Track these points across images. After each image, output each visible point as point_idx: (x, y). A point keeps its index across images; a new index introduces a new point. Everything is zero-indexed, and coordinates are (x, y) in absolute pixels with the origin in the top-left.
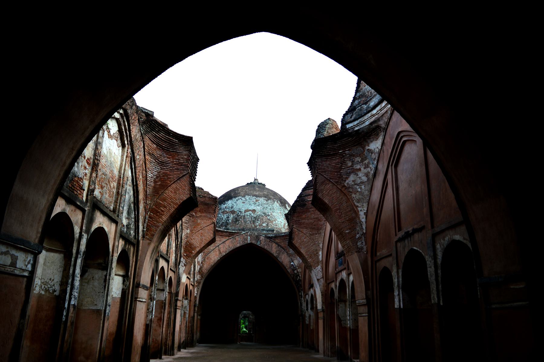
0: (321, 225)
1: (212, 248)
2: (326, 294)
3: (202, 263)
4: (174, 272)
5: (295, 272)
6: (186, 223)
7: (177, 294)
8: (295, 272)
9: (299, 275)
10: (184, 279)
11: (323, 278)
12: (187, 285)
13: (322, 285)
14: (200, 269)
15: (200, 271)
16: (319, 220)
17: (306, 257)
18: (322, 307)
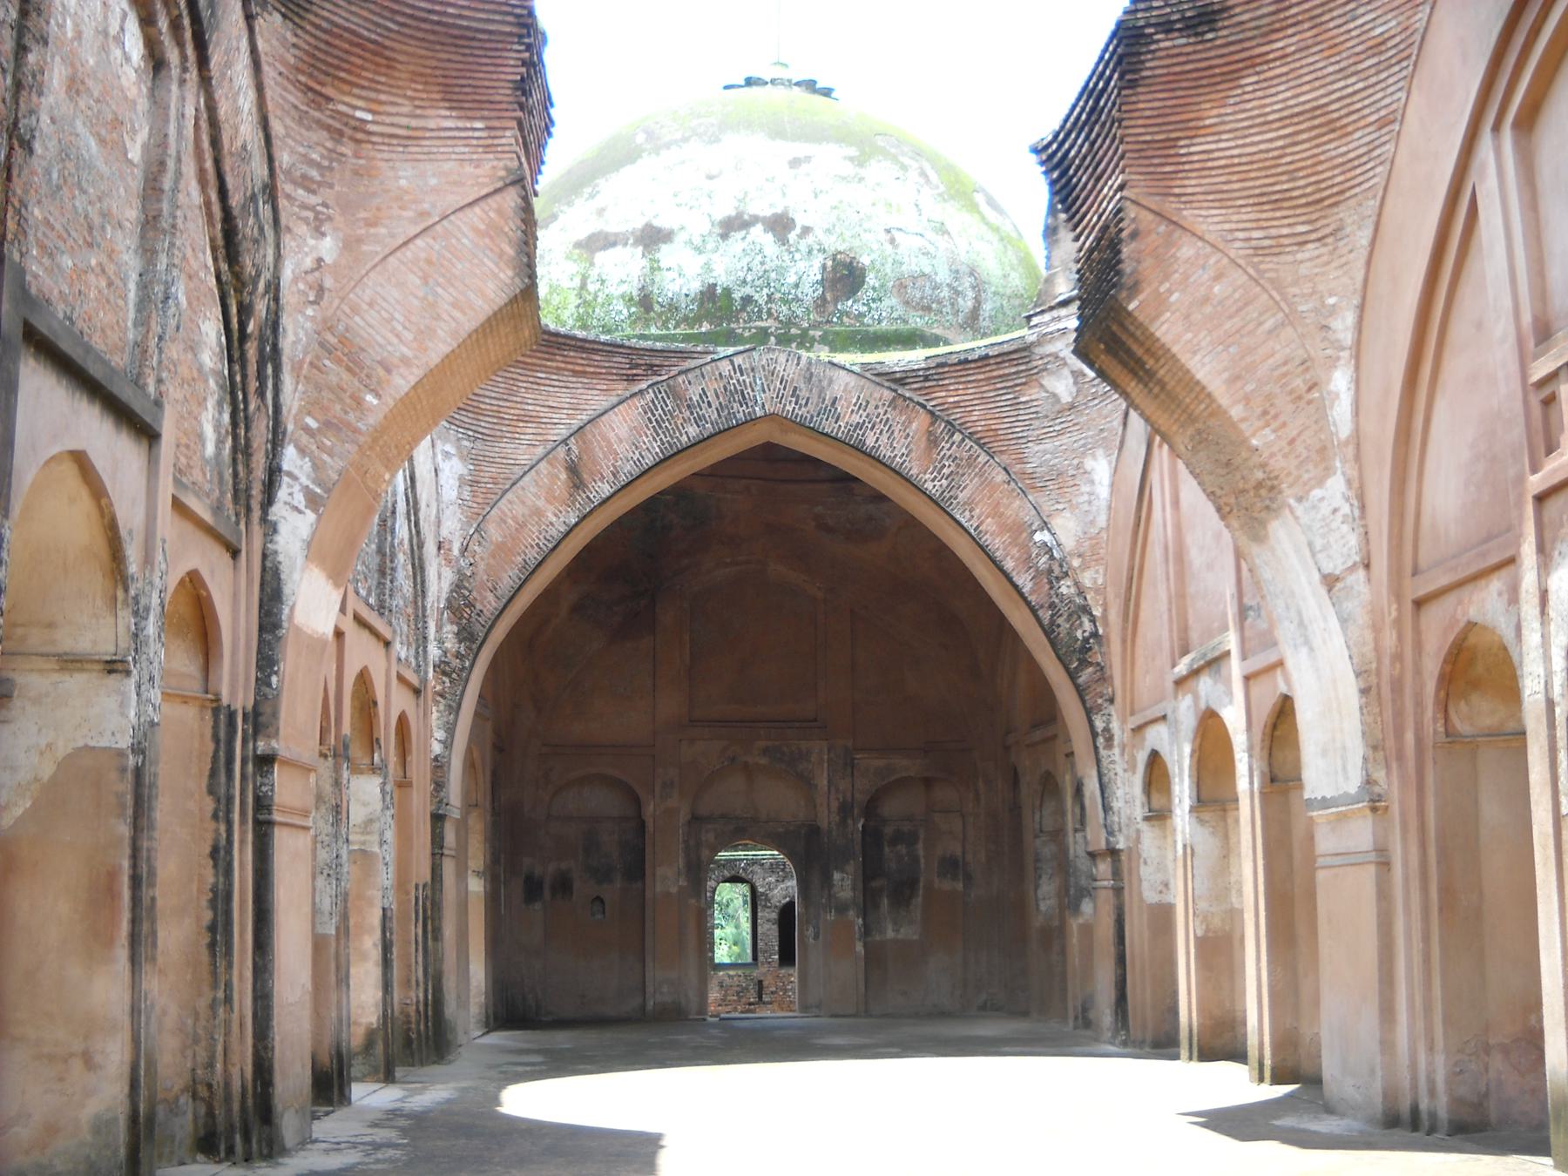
0: (1348, 165)
1: (525, 458)
2: (1397, 686)
3: (464, 550)
4: (235, 553)
5: (1066, 588)
6: (305, 183)
7: (260, 719)
8: (1066, 588)
9: (1086, 610)
10: (314, 604)
11: (1367, 566)
12: (363, 678)
13: (1362, 618)
14: (458, 587)
15: (460, 605)
16: (1331, 127)
17: (1236, 412)
18: (1369, 782)
